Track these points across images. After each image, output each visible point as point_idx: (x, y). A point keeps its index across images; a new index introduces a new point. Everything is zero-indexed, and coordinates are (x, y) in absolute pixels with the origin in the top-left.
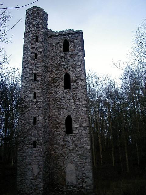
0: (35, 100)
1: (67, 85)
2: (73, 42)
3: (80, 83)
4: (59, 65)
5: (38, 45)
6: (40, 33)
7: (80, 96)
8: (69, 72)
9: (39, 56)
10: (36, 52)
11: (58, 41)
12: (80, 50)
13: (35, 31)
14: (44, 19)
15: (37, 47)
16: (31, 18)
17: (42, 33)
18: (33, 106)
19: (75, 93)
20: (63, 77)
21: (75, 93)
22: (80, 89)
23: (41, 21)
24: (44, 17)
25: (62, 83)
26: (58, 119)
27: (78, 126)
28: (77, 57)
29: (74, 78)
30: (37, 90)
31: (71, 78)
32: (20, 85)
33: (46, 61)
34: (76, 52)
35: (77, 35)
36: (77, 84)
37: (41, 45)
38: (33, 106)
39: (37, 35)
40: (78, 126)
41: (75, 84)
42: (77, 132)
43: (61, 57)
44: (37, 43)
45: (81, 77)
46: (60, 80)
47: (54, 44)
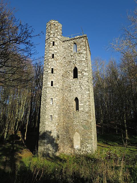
0: (52, 87)
1: (75, 76)
2: (80, 44)
3: (84, 74)
4: (70, 62)
5: (54, 48)
6: (56, 39)
7: (84, 83)
8: (77, 66)
9: (55, 56)
10: (53, 53)
11: (69, 45)
12: (85, 49)
13: (52, 38)
14: (59, 29)
15: (54, 49)
16: (49, 29)
17: (57, 39)
18: (51, 91)
19: (81, 81)
20: (73, 70)
21: (81, 81)
22: (85, 78)
23: (57, 31)
24: (59, 27)
25: (72, 74)
26: (69, 100)
27: (83, 104)
28: (82, 55)
29: (80, 70)
30: (54, 80)
31: (78, 71)
32: (20, 155)
33: (60, 59)
34: (81, 51)
35: (82, 39)
36: (82, 74)
37: (57, 48)
38: (51, 91)
39: (53, 41)
40: (83, 104)
41: (80, 74)
42: (82, 109)
43: (72, 56)
44: (53, 46)
45: (85, 69)
46: (70, 72)
47: (66, 47)
